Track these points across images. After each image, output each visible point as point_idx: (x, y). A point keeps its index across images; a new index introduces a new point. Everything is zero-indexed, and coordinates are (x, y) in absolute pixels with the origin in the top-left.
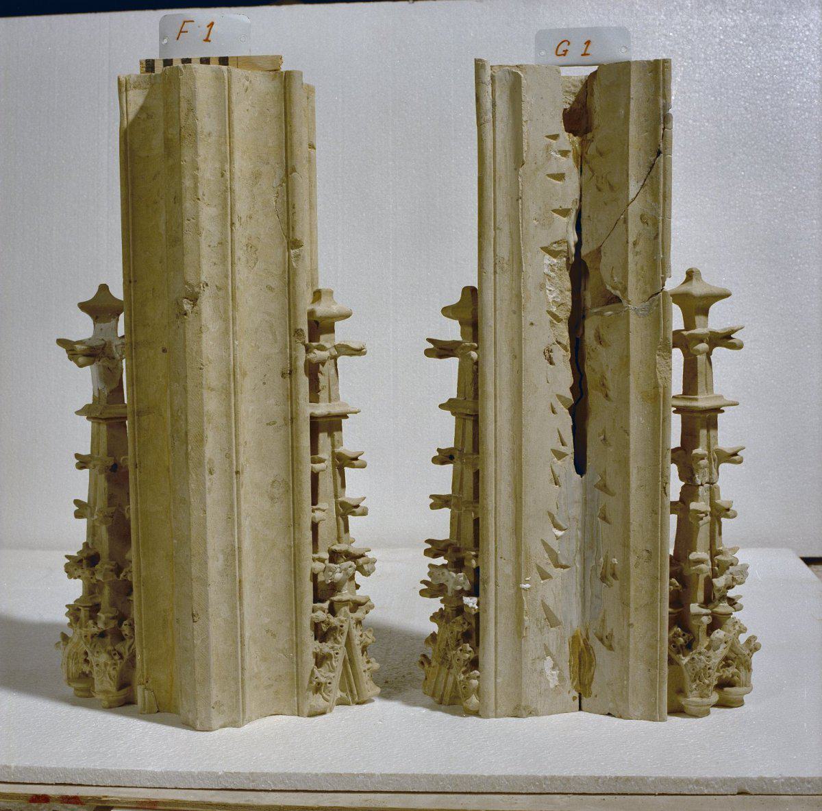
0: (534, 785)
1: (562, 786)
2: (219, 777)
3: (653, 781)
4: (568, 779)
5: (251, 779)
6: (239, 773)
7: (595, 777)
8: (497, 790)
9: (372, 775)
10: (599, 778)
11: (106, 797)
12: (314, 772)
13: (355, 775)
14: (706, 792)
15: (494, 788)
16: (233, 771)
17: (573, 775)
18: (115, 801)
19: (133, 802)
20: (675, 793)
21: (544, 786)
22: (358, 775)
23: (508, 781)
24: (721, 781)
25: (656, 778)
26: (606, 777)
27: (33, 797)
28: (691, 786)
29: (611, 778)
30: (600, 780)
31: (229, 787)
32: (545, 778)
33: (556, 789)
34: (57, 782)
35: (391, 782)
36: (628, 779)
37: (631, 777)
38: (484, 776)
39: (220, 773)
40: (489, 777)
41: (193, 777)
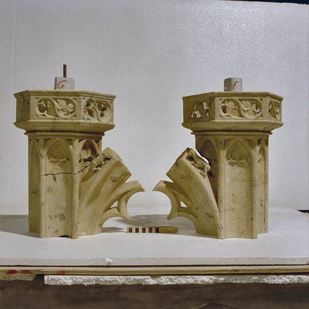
0: (223, 261)
1: (235, 261)
2: (89, 260)
3: (272, 259)
4: (237, 259)
5: (102, 261)
6: (97, 258)
7: (248, 258)
8: (208, 263)
9: (155, 258)
10: (250, 258)
11: (42, 270)
12: (130, 258)
13: (147, 258)
14: (294, 263)
15: (207, 263)
16: (94, 258)
17: (239, 257)
18: (46, 272)
19: (54, 272)
20: (281, 264)
21: (227, 262)
22: (149, 258)
23: (212, 260)
24: (300, 259)
25: (273, 258)
26: (253, 258)
27: (8, 271)
28: (288, 261)
29: (255, 258)
30: (250, 259)
31: (93, 265)
32: (228, 258)
33: (232, 263)
34: (16, 265)
35: (162, 261)
36: (262, 258)
37: (263, 258)
38: (203, 258)
39: (89, 259)
40: (204, 258)
41: (77, 260)
